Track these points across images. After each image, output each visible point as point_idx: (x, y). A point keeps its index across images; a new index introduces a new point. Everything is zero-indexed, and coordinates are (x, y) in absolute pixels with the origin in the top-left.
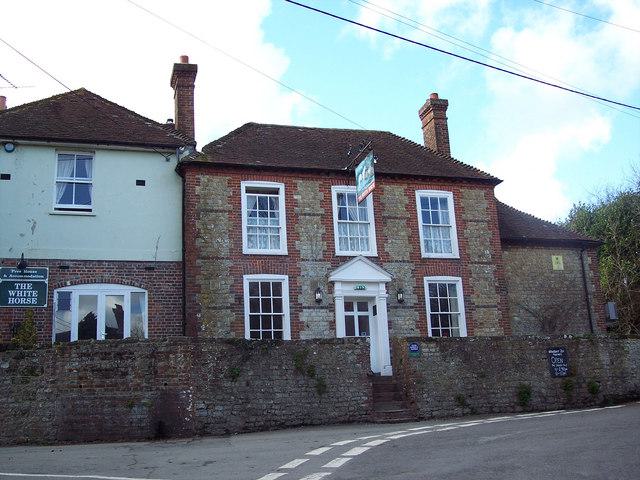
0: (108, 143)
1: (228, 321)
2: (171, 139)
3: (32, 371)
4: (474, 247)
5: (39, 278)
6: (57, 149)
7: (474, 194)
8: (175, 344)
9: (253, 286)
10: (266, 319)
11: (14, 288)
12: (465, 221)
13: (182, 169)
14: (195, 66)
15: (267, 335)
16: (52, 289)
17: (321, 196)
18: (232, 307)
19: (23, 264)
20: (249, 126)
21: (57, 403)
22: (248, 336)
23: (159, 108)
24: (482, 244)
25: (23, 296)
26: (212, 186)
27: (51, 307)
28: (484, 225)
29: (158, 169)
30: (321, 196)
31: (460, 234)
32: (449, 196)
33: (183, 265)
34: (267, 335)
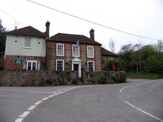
0: (34, 36)
1: (53, 67)
2: (45, 36)
3: (20, 74)
4: (97, 56)
5: (21, 59)
6: (25, 37)
7: (97, 47)
8: (44, 71)
9: (58, 62)
10: (60, 67)
11: (17, 60)
12: (95, 52)
13: (46, 41)
14: (50, 23)
15: (60, 70)
16: (23, 61)
17: (70, 46)
18: (54, 65)
19: (19, 56)
20: (59, 33)
21: (24, 80)
22: (57, 70)
23: (43, 29)
24: (98, 55)
25: (18, 62)
26: (51, 45)
27: (23, 64)
28: (99, 52)
29: (42, 41)
30: (70, 46)
31: (94, 54)
32: (93, 47)
33: (46, 58)
34: (60, 70)
